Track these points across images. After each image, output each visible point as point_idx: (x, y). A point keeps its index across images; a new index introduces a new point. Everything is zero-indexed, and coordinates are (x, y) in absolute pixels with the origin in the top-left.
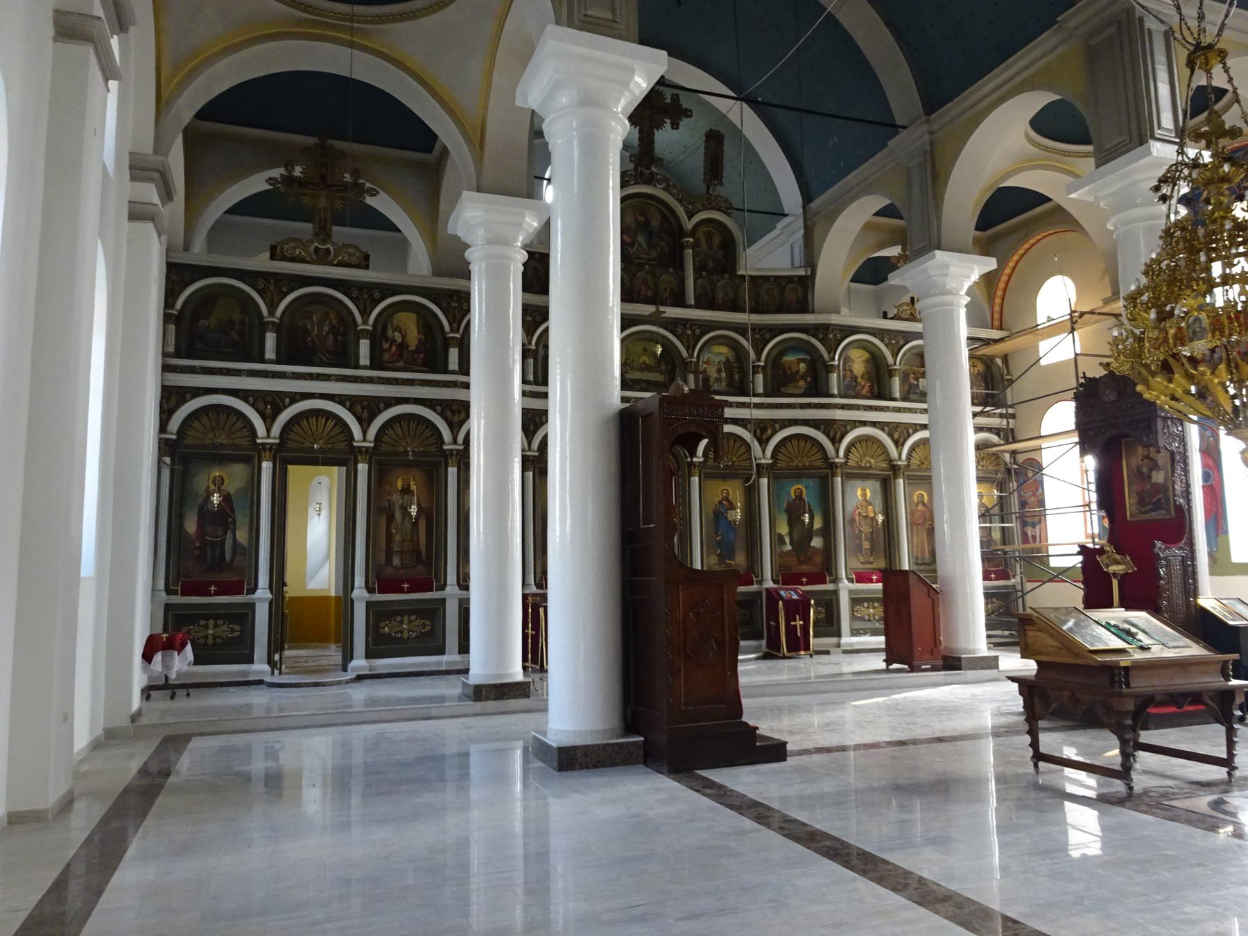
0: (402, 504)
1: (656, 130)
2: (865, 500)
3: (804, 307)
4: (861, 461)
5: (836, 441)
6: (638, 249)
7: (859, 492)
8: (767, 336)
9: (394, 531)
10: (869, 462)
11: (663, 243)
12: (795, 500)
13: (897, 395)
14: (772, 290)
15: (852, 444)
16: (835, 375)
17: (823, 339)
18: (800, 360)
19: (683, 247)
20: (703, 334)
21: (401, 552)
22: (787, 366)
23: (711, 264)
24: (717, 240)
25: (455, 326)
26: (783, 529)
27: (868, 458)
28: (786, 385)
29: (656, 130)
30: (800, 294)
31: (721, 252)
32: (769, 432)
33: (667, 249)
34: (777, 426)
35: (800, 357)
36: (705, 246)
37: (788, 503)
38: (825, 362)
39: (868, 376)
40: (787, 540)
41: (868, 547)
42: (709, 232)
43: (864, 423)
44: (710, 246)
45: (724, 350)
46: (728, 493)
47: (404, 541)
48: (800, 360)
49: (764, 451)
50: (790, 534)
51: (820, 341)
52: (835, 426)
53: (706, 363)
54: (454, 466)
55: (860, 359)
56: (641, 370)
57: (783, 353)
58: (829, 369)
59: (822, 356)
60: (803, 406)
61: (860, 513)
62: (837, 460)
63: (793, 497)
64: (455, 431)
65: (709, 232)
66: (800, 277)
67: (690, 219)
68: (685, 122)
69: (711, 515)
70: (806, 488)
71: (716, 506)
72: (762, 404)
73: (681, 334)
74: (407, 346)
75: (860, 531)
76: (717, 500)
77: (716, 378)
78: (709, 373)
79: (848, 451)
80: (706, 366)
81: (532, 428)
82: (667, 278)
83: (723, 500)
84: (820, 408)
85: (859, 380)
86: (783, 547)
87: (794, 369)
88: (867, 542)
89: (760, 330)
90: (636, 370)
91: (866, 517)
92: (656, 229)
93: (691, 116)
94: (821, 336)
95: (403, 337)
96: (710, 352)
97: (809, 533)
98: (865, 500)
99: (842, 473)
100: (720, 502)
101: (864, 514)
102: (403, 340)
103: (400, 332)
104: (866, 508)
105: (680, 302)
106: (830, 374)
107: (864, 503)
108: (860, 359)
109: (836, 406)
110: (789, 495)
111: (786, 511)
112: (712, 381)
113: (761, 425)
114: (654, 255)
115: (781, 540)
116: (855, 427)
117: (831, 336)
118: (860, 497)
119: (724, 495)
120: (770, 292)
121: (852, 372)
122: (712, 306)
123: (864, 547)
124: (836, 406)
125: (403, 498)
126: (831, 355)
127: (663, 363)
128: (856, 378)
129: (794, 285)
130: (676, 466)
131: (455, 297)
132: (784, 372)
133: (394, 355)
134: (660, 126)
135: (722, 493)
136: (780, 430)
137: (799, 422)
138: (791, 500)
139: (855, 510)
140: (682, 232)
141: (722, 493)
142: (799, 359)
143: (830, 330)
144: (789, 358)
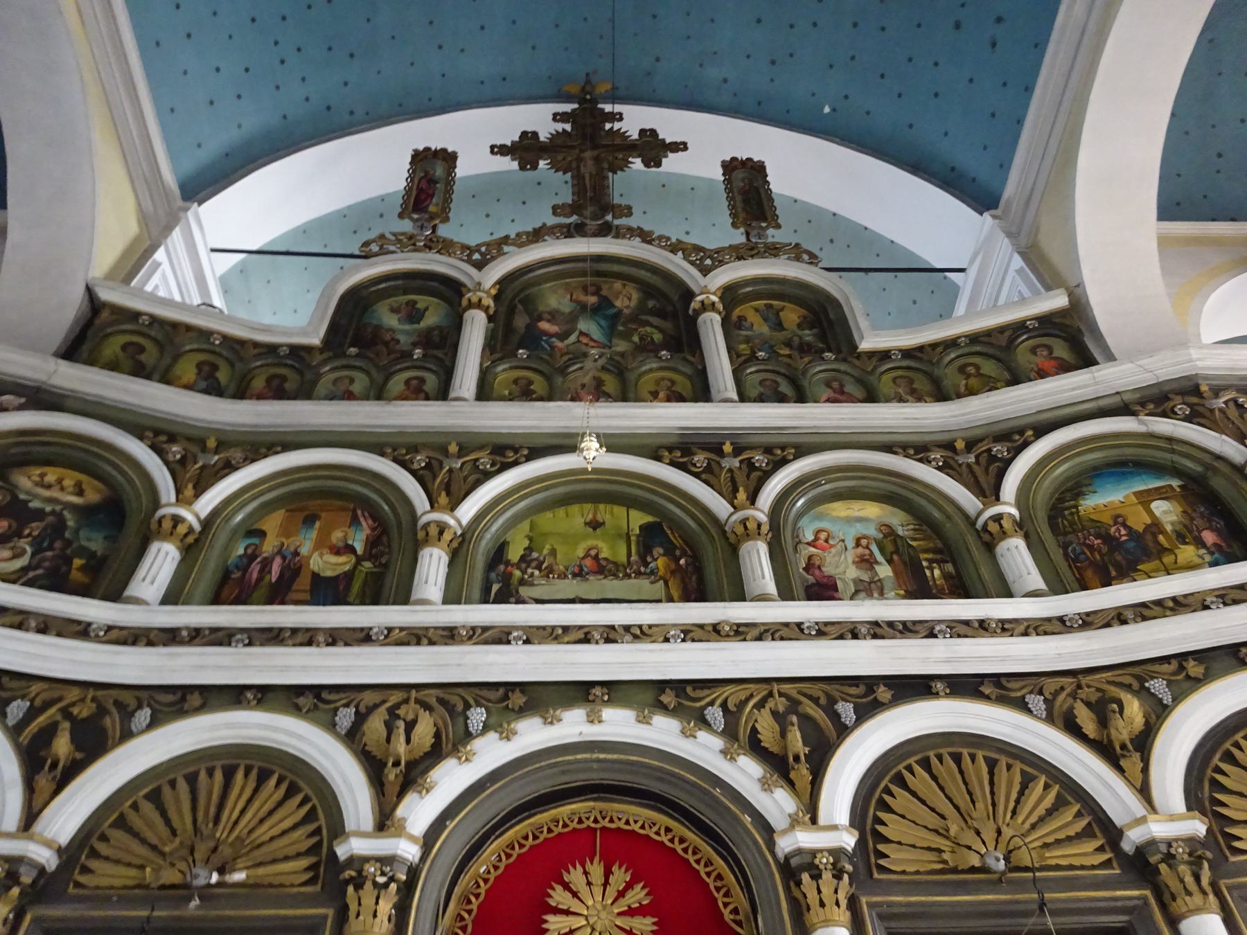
6: (579, 341)
8: (999, 449)
18: (1145, 498)
22: (1106, 519)
32: (1134, 709)
45: (872, 510)
49: (1144, 791)
56: (579, 574)
57: (1075, 487)
65: (769, 307)
77: (858, 581)
78: (828, 570)
80: (812, 550)
81: (62, 746)
87: (1139, 520)
89: (970, 445)
90: (563, 576)
96: (820, 517)
127: (658, 551)
130: (744, 904)
132: (1108, 539)
136: (1177, 699)
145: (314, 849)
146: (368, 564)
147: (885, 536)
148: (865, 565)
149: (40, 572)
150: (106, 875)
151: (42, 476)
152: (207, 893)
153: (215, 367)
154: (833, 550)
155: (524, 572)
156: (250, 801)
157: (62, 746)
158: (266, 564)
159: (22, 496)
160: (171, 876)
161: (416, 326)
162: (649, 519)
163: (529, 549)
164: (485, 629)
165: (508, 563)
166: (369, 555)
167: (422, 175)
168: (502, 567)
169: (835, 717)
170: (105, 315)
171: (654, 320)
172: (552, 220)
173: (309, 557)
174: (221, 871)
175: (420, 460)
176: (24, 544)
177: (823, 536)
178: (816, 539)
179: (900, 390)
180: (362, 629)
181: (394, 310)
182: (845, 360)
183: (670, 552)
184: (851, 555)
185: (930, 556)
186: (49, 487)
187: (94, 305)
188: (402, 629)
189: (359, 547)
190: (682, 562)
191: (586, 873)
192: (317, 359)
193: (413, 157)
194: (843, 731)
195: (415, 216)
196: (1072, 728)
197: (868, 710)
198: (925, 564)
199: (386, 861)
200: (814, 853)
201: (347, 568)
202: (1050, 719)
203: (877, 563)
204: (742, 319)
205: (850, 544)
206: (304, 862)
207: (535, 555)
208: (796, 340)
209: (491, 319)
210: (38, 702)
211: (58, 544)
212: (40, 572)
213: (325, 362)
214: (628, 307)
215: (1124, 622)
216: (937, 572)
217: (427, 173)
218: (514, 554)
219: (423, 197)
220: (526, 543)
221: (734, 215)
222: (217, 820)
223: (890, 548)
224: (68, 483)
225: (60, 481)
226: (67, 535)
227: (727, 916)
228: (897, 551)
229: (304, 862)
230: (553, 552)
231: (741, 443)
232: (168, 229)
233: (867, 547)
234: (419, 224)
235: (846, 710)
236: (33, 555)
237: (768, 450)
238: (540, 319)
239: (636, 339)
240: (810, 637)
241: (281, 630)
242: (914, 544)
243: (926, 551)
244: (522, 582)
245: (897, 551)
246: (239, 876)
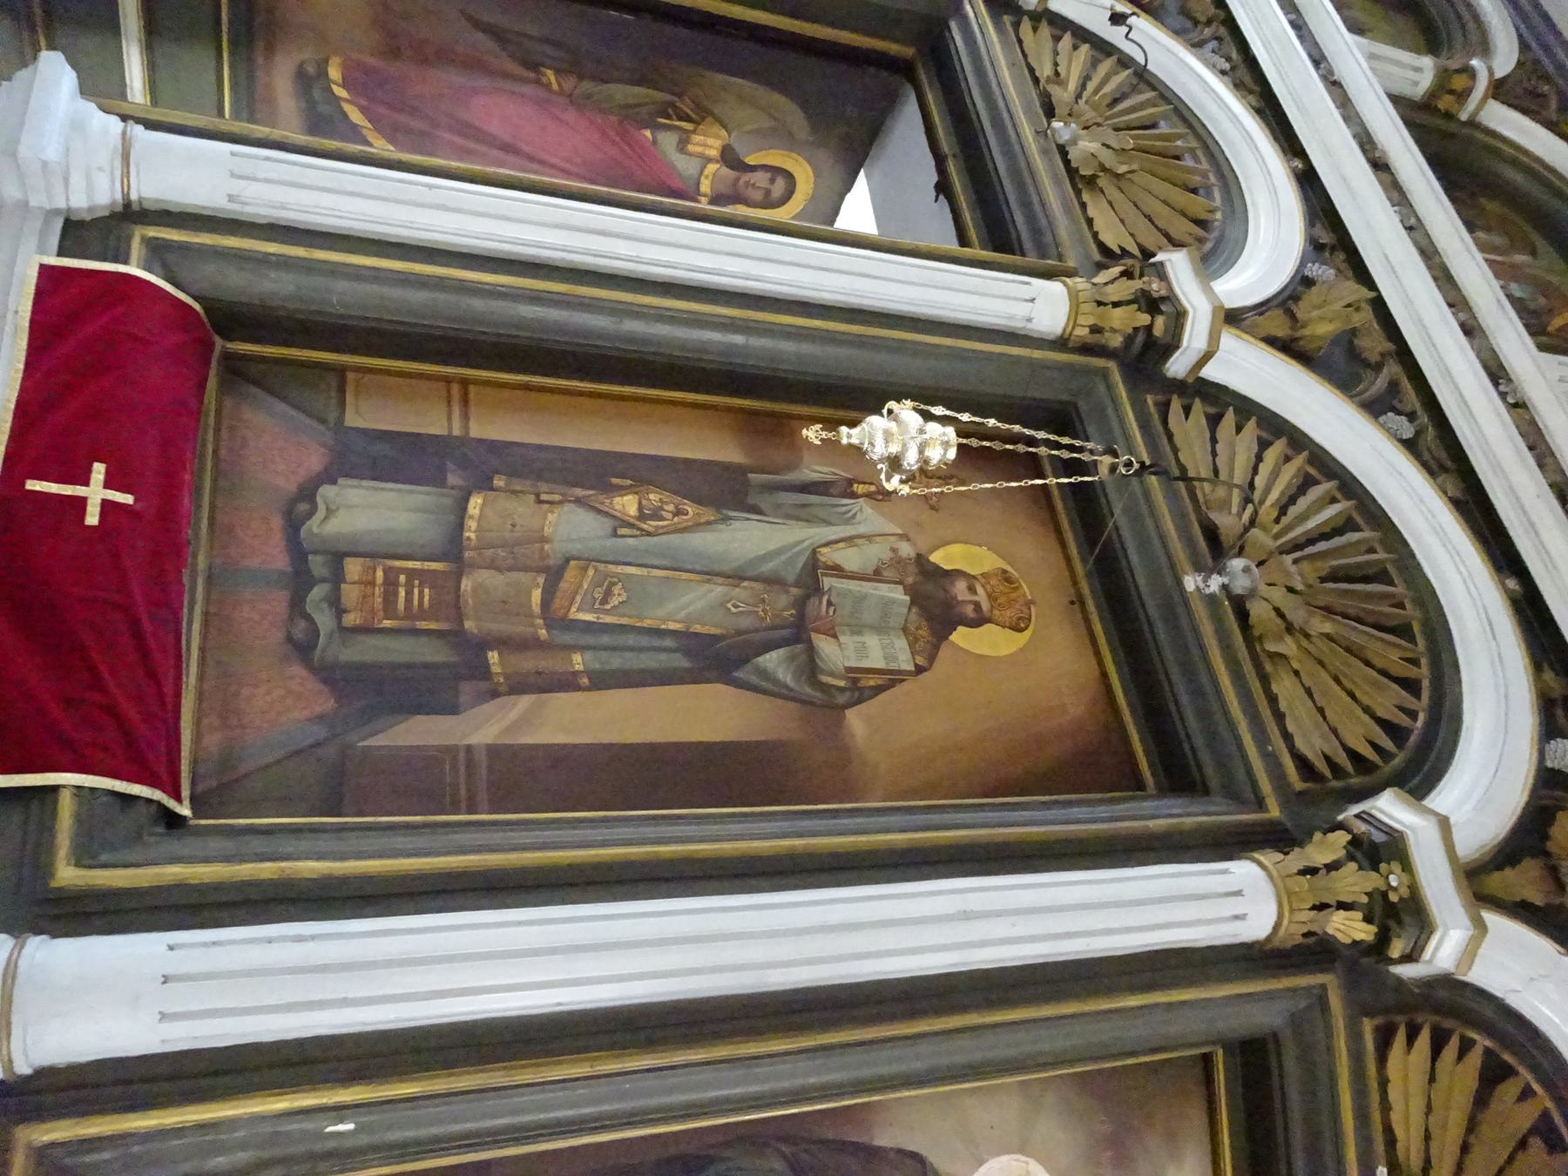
0: (837, 571)
9: (627, 504)
21: (453, 550)
47: (554, 575)
54: (1285, 897)
125: (876, 576)
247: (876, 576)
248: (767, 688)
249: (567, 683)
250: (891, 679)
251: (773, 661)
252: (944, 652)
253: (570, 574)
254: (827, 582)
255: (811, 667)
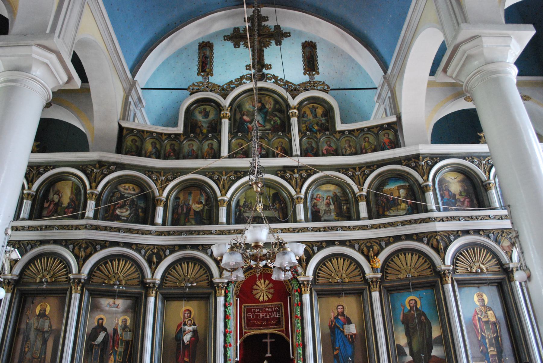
0: (37, 326)
1: (264, 48)
2: (484, 306)
3: (396, 144)
4: (471, 267)
5: (441, 252)
7: (476, 298)
8: (367, 171)
9: (27, 349)
10: (480, 268)
11: (276, 118)
12: (410, 311)
13: (497, 205)
14: (368, 139)
15: (459, 252)
16: (431, 193)
17: (416, 166)
18: (399, 188)
19: (289, 118)
20: (309, 176)
23: (316, 128)
24: (320, 111)
25: (94, 184)
26: (402, 340)
27: (477, 264)
28: (389, 209)
29: (264, 48)
30: (391, 137)
31: (324, 118)
33: (279, 122)
34: (383, 243)
35: (399, 185)
36: (311, 117)
37: (404, 314)
38: (419, 185)
39: (466, 193)
40: (407, 351)
41: (495, 353)
42: (313, 107)
43: (467, 232)
44: (315, 116)
45: (332, 187)
46: (343, 308)
47: (34, 358)
48: (399, 188)
50: (410, 344)
51: (413, 168)
52: (438, 237)
53: (315, 199)
55: (456, 180)
58: (424, 190)
59: (417, 181)
60: (403, 223)
61: (480, 319)
62: (443, 268)
63: (409, 308)
64: (81, 263)
65: (313, 107)
66: (389, 124)
67: (294, 98)
68: (285, 42)
69: (328, 331)
70: (420, 298)
71: (332, 321)
72: (367, 226)
73: (290, 178)
74: (62, 204)
75: (483, 337)
76: (332, 316)
77: (325, 210)
78: (318, 207)
79: (455, 260)
80: (316, 201)
81: (155, 260)
82: (276, 141)
83: (338, 314)
84: (420, 223)
85: (457, 197)
86: (404, 358)
88: (492, 348)
89: (360, 168)
91: (487, 322)
92: (270, 110)
93: (290, 36)
94: (413, 164)
95: (60, 198)
97: (429, 345)
98: (484, 306)
99: (452, 278)
100: (336, 318)
101: (484, 320)
102: (59, 200)
103: (58, 195)
104: (486, 313)
105: (288, 152)
106: (426, 194)
107: (483, 309)
108: (456, 180)
109: (435, 219)
110: (404, 306)
111: (403, 323)
112: (322, 213)
113: (369, 244)
114: (268, 126)
115: (400, 351)
116: (459, 236)
117: (423, 163)
118: (478, 303)
119: (339, 310)
120: (367, 139)
121: (449, 191)
122: (316, 155)
123: (490, 354)
124: (435, 219)
125: (38, 322)
126: (425, 177)
127: (277, 202)
128: (454, 195)
129: (385, 131)
131: (97, 166)
133: (50, 211)
134: (267, 45)
135: (337, 309)
137: (403, 237)
138: (406, 311)
139: (474, 316)
140: (288, 107)
141: (337, 309)
142: (398, 187)
143: (421, 158)
144: (391, 187)
145: (208, 279)
146: (206, 207)
147: (334, 196)
148: (328, 205)
149: (133, 214)
150: (169, 284)
151: (125, 186)
152: (189, 288)
153: (156, 144)
154: (320, 201)
155: (244, 209)
156: (193, 269)
157: (155, 260)
158: (182, 207)
159: (123, 194)
160: (183, 285)
161: (207, 119)
162: (274, 192)
163: (245, 202)
164: (237, 230)
165: (240, 206)
166: (206, 204)
167: (203, 55)
168: (239, 207)
169: (313, 250)
170: (125, 131)
171: (278, 114)
172: (245, 72)
173: (192, 205)
174: (191, 283)
175: (216, 177)
176: (127, 207)
177: (318, 197)
178: (317, 197)
179: (346, 145)
180: (210, 231)
181: (200, 113)
182: (332, 135)
183: (280, 203)
184: (325, 202)
185: (344, 202)
186: (127, 190)
187: (121, 128)
188: (219, 230)
189: (203, 202)
190: (283, 205)
191: (260, 282)
192: (182, 138)
193: (199, 46)
194: (314, 254)
195: (203, 74)
196: (363, 253)
197: (320, 248)
198: (343, 205)
199: (223, 283)
200: (304, 281)
201: (201, 208)
202: (358, 251)
203: (331, 204)
204: (305, 113)
205: (325, 199)
206: (207, 281)
207: (247, 203)
208: (320, 122)
209: (230, 119)
210: (146, 249)
211: (134, 206)
212: (133, 214)
213: (185, 140)
214: (270, 108)
215: (380, 228)
216: (345, 207)
217: (204, 53)
218: (242, 203)
219: (204, 65)
220: (244, 200)
221: (305, 69)
222: (188, 273)
223: (335, 200)
224: (131, 188)
225: (129, 187)
226: (135, 203)
227: (288, 290)
228: (336, 201)
229: (207, 281)
230: (251, 203)
231: (299, 168)
232: (130, 90)
233: (329, 200)
234: (204, 77)
235: (315, 249)
236: (130, 210)
237: (306, 171)
238: (244, 115)
239: (272, 123)
240: (310, 231)
241: (192, 231)
242: (341, 198)
243: (343, 201)
244: (244, 212)
245: (336, 201)
246: (195, 284)
247: (38, 322)
248: (48, 337)
249: (45, 357)
250: (50, 323)
251: (46, 336)
252: (49, 316)
253: (34, 356)
254: (38, 328)
255: (47, 332)
